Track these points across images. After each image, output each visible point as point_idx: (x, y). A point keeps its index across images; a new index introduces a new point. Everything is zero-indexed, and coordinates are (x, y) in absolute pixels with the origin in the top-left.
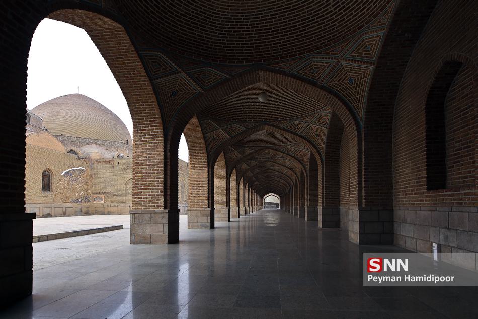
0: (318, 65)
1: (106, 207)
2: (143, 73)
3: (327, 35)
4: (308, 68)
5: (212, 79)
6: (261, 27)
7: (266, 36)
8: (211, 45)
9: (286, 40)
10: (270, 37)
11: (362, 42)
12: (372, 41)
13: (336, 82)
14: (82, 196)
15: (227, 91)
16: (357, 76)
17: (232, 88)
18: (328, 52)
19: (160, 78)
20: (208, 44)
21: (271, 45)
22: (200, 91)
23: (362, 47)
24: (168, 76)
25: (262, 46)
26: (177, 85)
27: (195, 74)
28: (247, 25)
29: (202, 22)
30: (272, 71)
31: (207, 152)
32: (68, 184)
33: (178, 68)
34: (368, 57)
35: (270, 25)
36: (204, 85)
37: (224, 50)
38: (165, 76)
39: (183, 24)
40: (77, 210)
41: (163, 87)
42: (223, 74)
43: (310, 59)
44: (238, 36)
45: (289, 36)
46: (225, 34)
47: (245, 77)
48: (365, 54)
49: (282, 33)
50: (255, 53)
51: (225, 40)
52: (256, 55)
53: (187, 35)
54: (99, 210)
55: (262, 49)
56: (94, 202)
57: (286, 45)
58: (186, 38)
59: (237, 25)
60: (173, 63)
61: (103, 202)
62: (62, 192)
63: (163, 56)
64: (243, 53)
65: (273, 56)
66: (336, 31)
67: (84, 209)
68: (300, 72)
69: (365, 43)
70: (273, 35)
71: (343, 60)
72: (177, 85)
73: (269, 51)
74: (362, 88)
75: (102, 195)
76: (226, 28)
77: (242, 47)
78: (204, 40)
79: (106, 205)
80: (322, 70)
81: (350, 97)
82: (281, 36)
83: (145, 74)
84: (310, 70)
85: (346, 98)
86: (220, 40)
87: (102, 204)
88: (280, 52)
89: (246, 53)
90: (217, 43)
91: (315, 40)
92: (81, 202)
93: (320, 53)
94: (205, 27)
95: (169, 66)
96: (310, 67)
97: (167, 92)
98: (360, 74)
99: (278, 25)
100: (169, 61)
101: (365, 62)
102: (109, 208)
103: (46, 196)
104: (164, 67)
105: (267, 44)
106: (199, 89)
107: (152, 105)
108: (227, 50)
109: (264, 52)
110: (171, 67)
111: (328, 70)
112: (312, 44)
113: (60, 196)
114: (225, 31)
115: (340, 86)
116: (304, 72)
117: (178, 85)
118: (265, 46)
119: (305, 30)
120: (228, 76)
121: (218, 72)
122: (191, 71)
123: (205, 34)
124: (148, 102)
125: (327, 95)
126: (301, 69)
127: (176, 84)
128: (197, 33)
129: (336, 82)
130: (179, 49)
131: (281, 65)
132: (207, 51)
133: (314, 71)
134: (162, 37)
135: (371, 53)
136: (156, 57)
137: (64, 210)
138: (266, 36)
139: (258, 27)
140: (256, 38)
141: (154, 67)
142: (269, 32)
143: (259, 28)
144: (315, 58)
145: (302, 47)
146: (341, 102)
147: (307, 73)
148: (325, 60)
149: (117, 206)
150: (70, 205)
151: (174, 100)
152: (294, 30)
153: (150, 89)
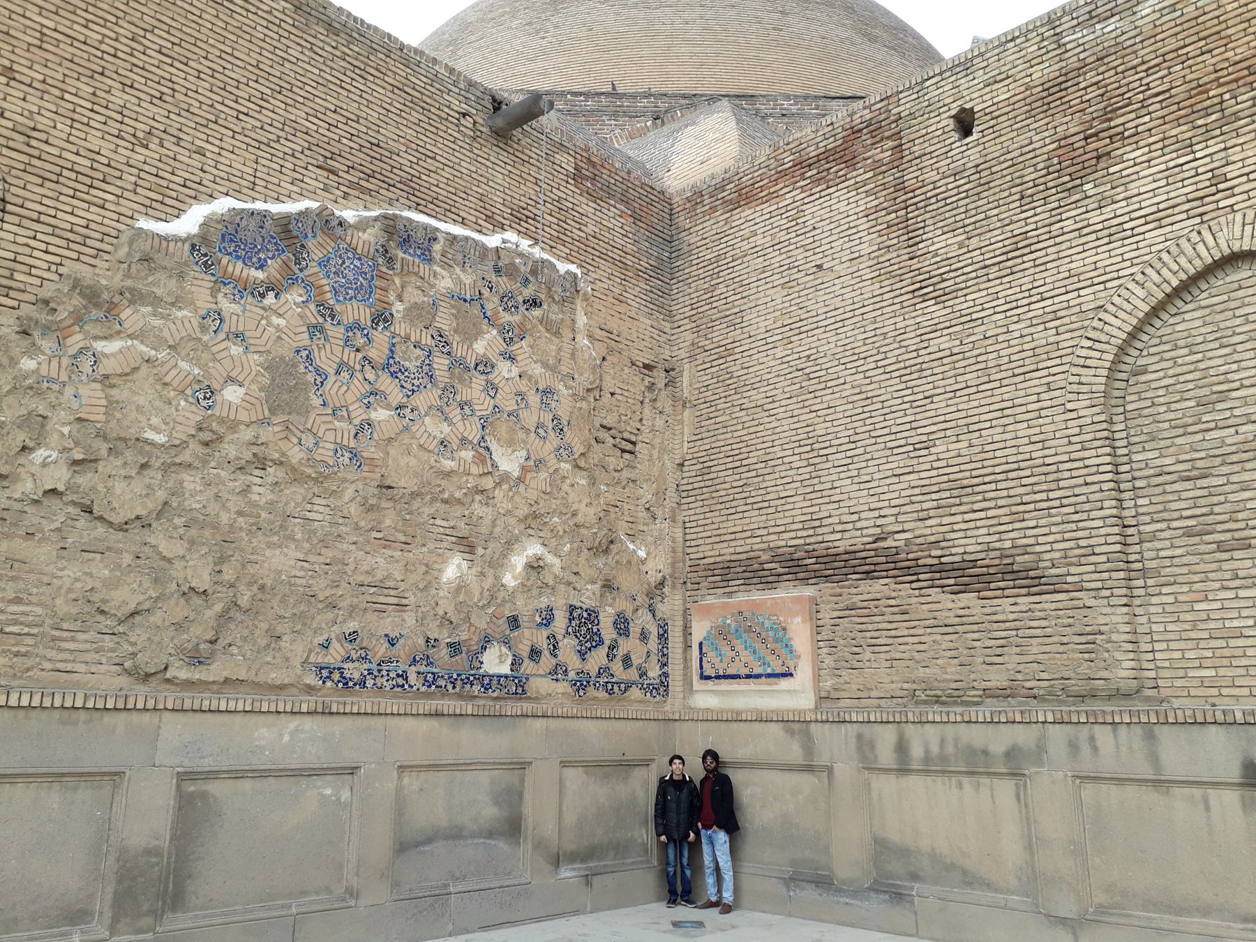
1: (845, 770)
14: (525, 607)
56: (707, 698)
61: (796, 696)
62: (127, 495)
75: (787, 593)
79: (834, 744)
87: (794, 724)
92: (515, 685)
102: (886, 786)
149: (1015, 765)
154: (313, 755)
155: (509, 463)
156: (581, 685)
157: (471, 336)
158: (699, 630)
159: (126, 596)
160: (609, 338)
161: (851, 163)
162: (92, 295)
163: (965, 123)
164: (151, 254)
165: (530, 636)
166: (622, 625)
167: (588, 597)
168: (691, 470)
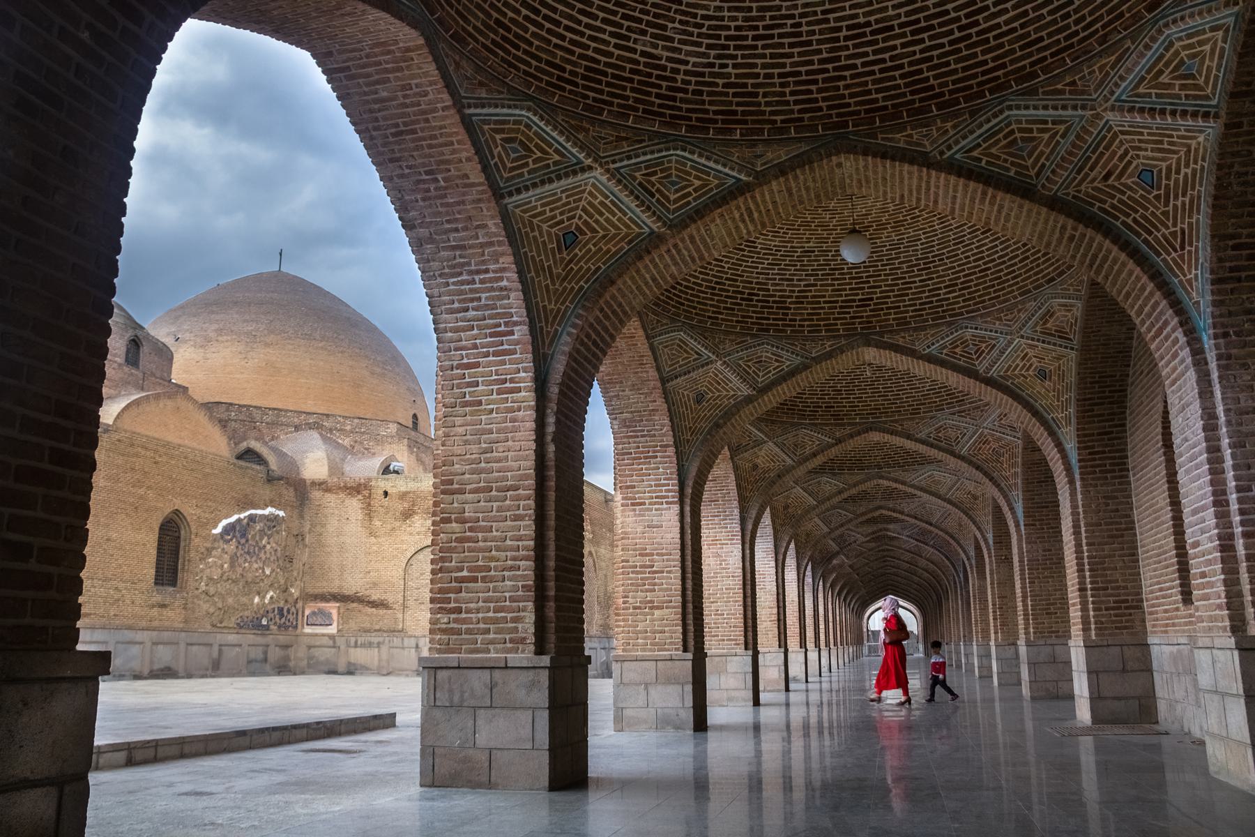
0: (1031, 130)
1: (342, 647)
2: (477, 177)
3: (1050, 35)
4: (999, 140)
5: (690, 189)
6: (837, 20)
7: (855, 46)
8: (683, 82)
9: (918, 56)
10: (869, 49)
11: (1167, 49)
12: (1201, 43)
13: (1095, 184)
14: (270, 608)
15: (742, 226)
16: (1163, 160)
17: (756, 215)
18: (1059, 86)
19: (527, 189)
20: (675, 80)
21: (873, 72)
22: (654, 227)
23: (1167, 65)
24: (551, 181)
25: (844, 78)
26: (579, 212)
27: (637, 174)
28: (792, 17)
29: (656, 16)
30: (884, 154)
31: (677, 445)
32: (232, 565)
33: (581, 156)
34: (1196, 97)
35: (865, 15)
36: (668, 210)
37: (727, 94)
38: (543, 183)
39: (598, 23)
40: (252, 656)
41: (535, 221)
42: (727, 170)
43: (1001, 112)
44: (767, 51)
45: (928, 43)
46: (726, 47)
47: (796, 177)
48: (1183, 87)
49: (904, 35)
50: (824, 99)
51: (726, 66)
52: (829, 108)
53: (610, 55)
54: (322, 659)
55: (847, 87)
56: (308, 630)
57: (920, 71)
58: (606, 64)
59: (763, 18)
60: (568, 140)
61: (332, 630)
62: (212, 590)
63: (535, 119)
64: (787, 103)
65: (885, 108)
66: (1077, 22)
67: (275, 654)
68: (975, 154)
69: (1177, 53)
70: (876, 42)
71: (1113, 109)
72: (579, 212)
73: (869, 92)
74: (1187, 200)
76: (729, 28)
77: (782, 85)
78: (664, 68)
79: (341, 642)
80: (1047, 145)
81: (1150, 233)
82: (904, 46)
83: (481, 179)
84: (1005, 147)
85: (1138, 235)
86: (712, 65)
87: (332, 637)
88: (904, 95)
89: (796, 103)
90: (702, 75)
91: (1013, 51)
92: (267, 627)
93: (1032, 92)
94: (664, 28)
95: (557, 151)
96: (1005, 137)
97: (549, 234)
98: (1175, 152)
99: (891, 13)
100: (554, 134)
101: (1184, 113)
102: (352, 650)
103: (163, 606)
104: (539, 154)
105: (860, 70)
106: (650, 223)
107: (501, 279)
108: (735, 95)
109: (852, 96)
110: (562, 155)
111: (1065, 145)
112: (1004, 66)
113: (205, 606)
114: (727, 38)
115: (1113, 197)
116: (991, 155)
117: (584, 210)
118: (853, 77)
119: (977, 23)
120: (742, 177)
121: (711, 164)
122: (625, 163)
123: (664, 48)
124: (487, 271)
125: (1075, 229)
126: (979, 145)
127: (577, 208)
128: (639, 48)
129: (1095, 184)
130: (587, 97)
131: (910, 136)
132: (674, 99)
133: (1021, 149)
134: (534, 63)
135: (1201, 81)
136: (515, 122)
137: (215, 655)
138: (855, 46)
139: (827, 21)
140: (825, 55)
141: (508, 155)
142: (864, 35)
143: (832, 24)
144: (1018, 107)
145: (975, 76)
146: (1122, 249)
147: (998, 158)
148: (1051, 112)
150: (232, 638)
151: (571, 261)
152: (941, 25)
153: (494, 225)
154: (235, 642)
155: (268, 572)
156: (279, 627)
157: (261, 539)
158: (307, 612)
159: (212, 610)
160: (288, 530)
161: (359, 493)
162: (207, 549)
163: (386, 494)
164: (215, 539)
165: (271, 615)
166: (288, 611)
167: (281, 605)
168: (307, 566)
